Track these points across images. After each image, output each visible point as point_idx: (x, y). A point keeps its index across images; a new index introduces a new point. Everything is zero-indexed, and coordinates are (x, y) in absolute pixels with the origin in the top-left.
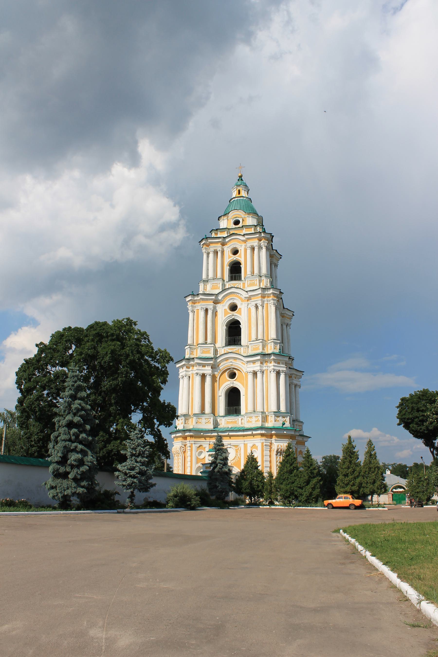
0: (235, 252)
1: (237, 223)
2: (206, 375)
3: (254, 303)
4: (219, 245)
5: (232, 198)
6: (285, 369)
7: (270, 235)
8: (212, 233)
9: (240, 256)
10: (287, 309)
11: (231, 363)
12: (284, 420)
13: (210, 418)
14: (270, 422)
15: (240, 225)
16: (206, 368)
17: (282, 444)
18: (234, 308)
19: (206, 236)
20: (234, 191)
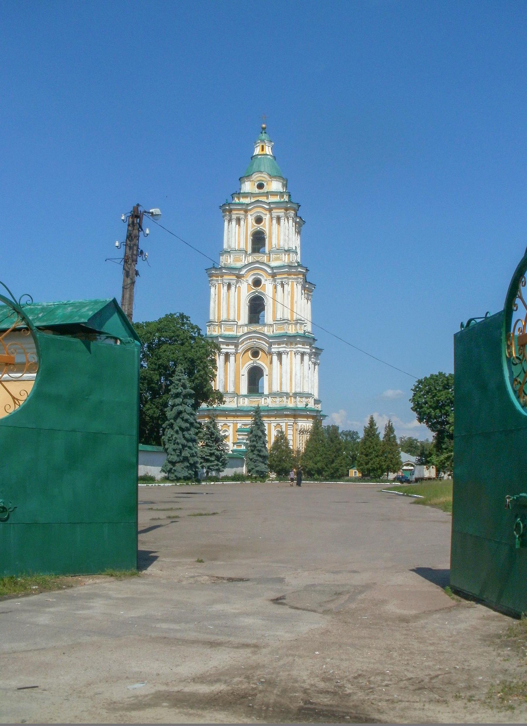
0: (259, 220)
1: (260, 186)
2: (230, 355)
3: (279, 281)
4: (242, 212)
5: (254, 155)
6: (309, 351)
7: (297, 205)
8: (233, 196)
9: (264, 226)
10: (309, 282)
11: (255, 343)
12: (307, 401)
13: (234, 398)
14: (294, 402)
15: (265, 190)
16: (230, 347)
17: (304, 424)
18: (257, 283)
19: (227, 200)
20: (257, 147)
